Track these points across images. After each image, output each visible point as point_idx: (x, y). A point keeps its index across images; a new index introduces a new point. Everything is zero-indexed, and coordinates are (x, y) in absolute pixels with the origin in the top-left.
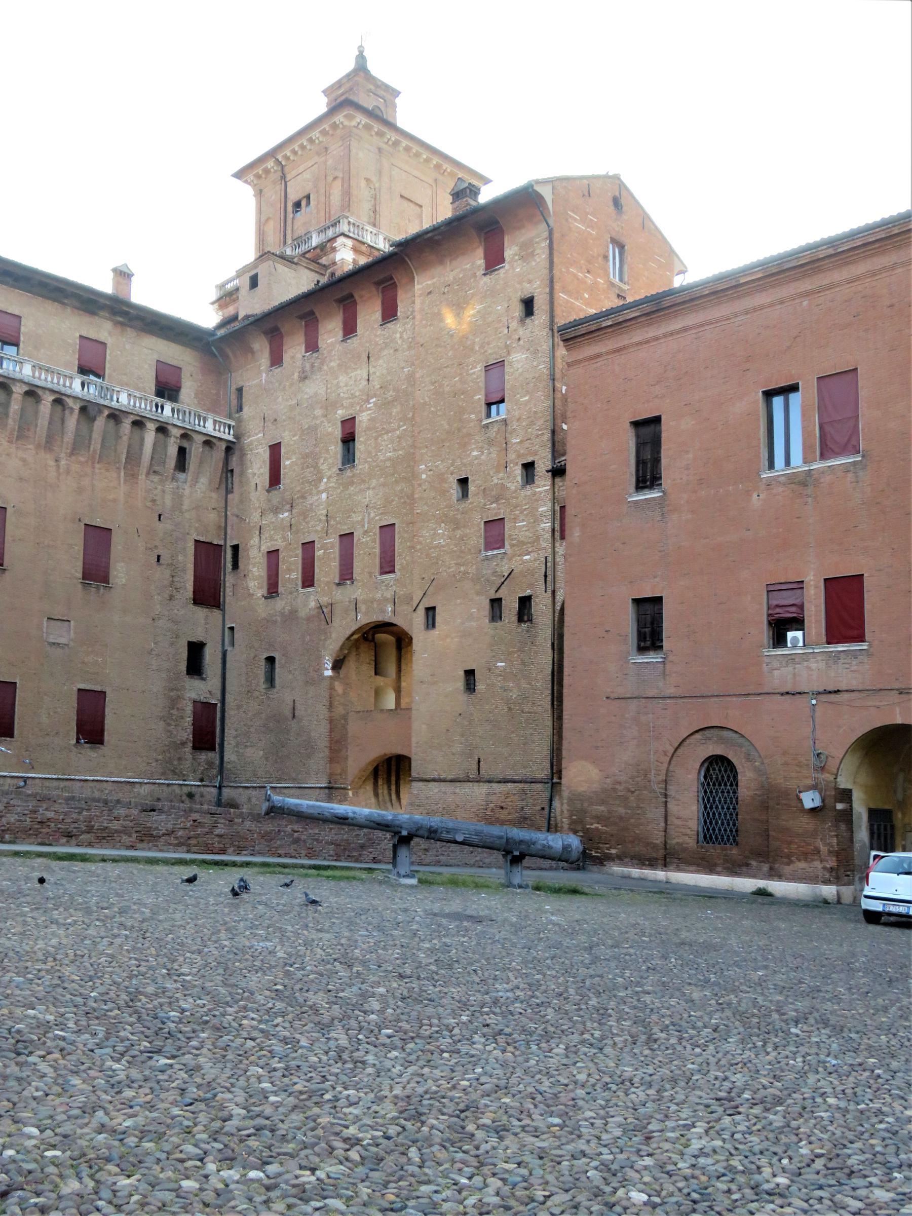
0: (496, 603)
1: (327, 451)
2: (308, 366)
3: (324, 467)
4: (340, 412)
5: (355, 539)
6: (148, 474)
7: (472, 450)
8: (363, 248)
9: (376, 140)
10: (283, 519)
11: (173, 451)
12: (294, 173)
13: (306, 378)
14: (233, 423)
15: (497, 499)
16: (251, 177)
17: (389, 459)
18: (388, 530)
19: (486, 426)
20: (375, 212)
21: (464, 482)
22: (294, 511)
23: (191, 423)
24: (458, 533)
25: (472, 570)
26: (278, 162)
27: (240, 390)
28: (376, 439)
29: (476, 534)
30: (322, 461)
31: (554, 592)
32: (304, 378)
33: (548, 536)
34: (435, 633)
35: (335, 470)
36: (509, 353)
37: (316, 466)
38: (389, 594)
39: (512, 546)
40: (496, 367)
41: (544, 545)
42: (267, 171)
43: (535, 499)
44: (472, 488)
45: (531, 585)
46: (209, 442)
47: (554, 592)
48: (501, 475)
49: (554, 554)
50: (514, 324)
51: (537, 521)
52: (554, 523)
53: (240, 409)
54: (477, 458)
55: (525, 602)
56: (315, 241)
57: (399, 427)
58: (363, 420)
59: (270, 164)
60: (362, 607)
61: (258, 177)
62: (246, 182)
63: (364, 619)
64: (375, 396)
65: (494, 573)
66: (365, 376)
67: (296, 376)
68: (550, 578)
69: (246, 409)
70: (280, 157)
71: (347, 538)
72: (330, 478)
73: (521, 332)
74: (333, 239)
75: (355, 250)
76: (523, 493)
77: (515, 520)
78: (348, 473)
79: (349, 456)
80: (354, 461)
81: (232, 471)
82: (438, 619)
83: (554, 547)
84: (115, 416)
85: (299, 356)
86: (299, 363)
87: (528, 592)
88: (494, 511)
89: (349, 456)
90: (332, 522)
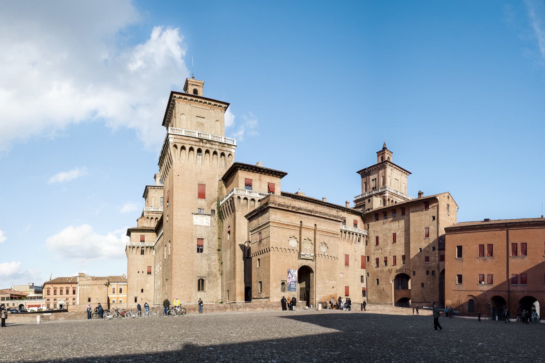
0: (428, 273)
8: (390, 193)
9: (391, 167)
12: (372, 173)
16: (361, 173)
20: (390, 183)
24: (420, 258)
25: (423, 265)
26: (368, 171)
29: (423, 259)
31: (439, 270)
33: (438, 260)
39: (431, 261)
41: (437, 262)
42: (365, 172)
43: (435, 254)
45: (434, 269)
47: (439, 270)
49: (439, 263)
51: (436, 257)
52: (439, 258)
54: (423, 245)
55: (433, 272)
56: (380, 191)
59: (366, 171)
61: (362, 173)
62: (360, 174)
65: (427, 266)
68: (438, 268)
70: (369, 170)
74: (385, 191)
75: (389, 193)
76: (433, 252)
77: (431, 257)
83: (439, 262)
87: (434, 270)
88: (427, 255)
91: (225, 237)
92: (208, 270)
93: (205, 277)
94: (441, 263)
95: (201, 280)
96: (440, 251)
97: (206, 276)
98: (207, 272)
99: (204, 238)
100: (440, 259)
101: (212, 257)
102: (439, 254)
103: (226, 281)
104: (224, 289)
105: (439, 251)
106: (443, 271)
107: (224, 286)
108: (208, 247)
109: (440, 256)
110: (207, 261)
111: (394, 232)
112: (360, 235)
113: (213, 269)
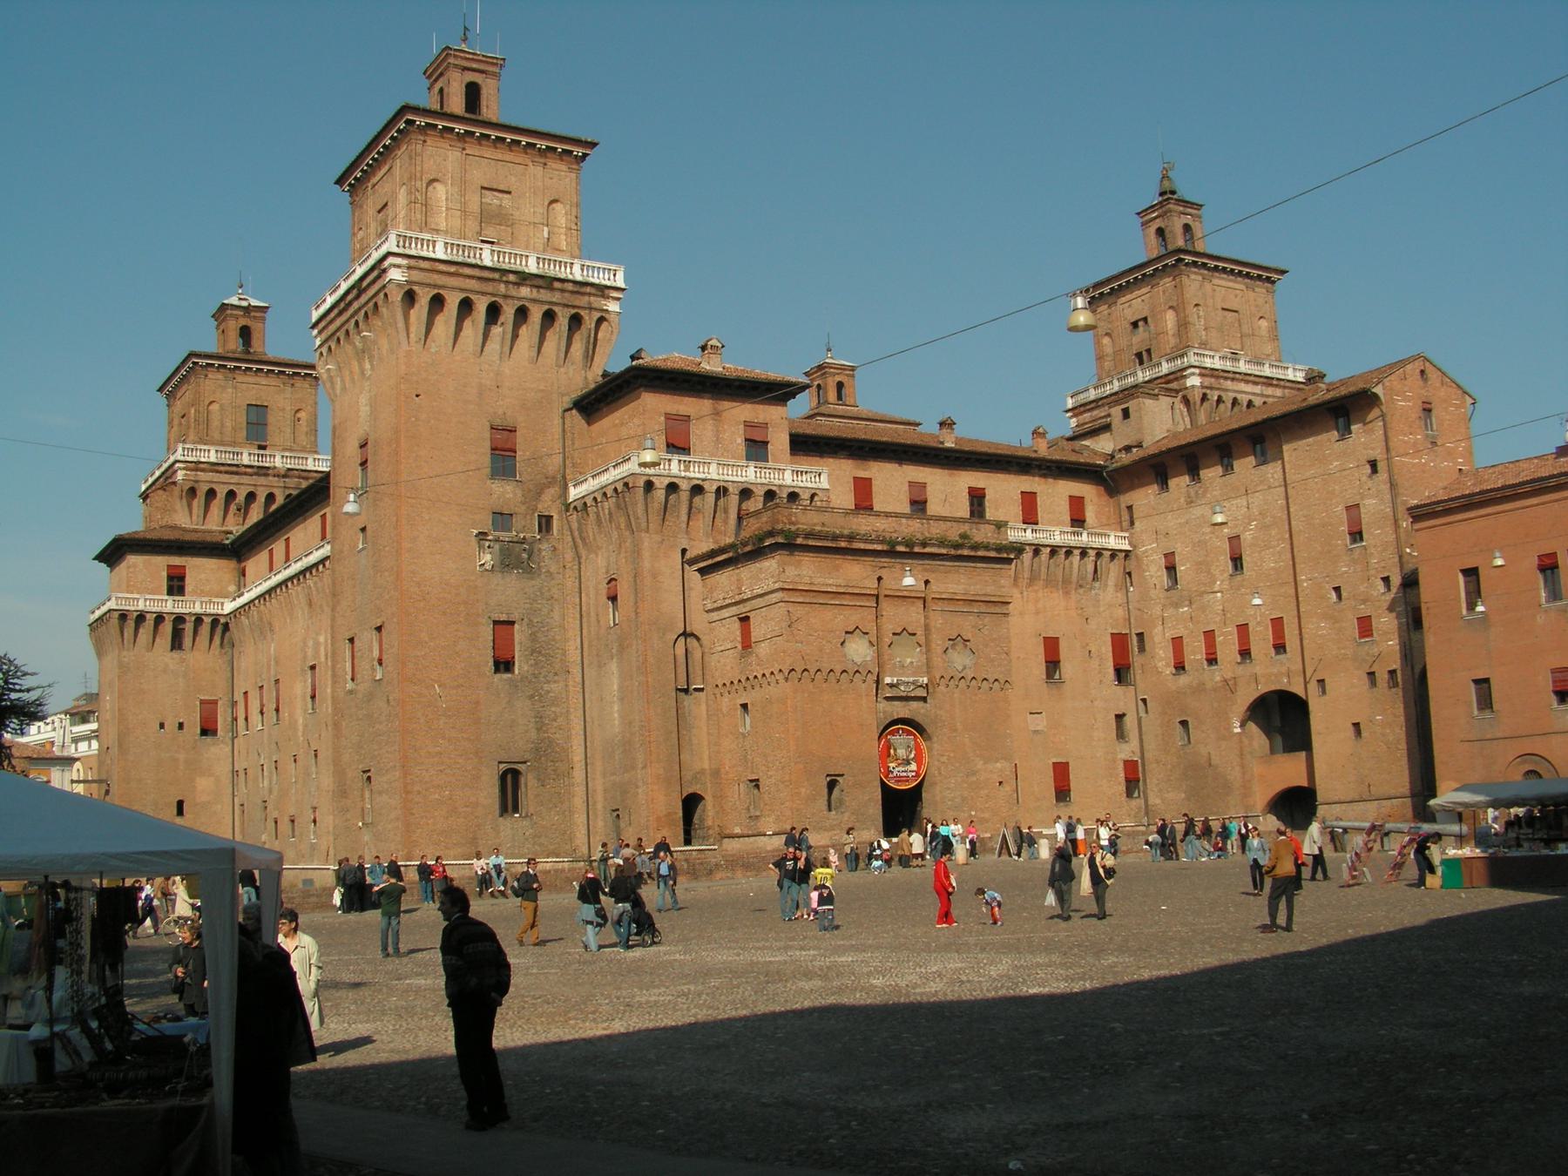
1: (1218, 560)
2: (1193, 493)
3: (1216, 573)
4: (1226, 530)
5: (1250, 629)
6: (1076, 589)
7: (1342, 567)
10: (1183, 613)
11: (1090, 568)
13: (1192, 502)
14: (1127, 535)
15: (1364, 601)
17: (1273, 568)
18: (1277, 623)
19: (1351, 550)
21: (1337, 590)
22: (1194, 606)
23: (1098, 542)
27: (1130, 508)
28: (1260, 552)
30: (1214, 567)
32: (1190, 502)
34: (1326, 697)
35: (1226, 575)
36: (1362, 499)
37: (1209, 572)
38: (1284, 669)
40: (1353, 509)
44: (1344, 594)
46: (1114, 554)
48: (1366, 585)
50: (1364, 478)
52: (1407, 618)
53: (1132, 523)
57: (1279, 545)
58: (1247, 537)
60: (1262, 680)
63: (1263, 688)
64: (1255, 520)
66: (1245, 504)
67: (1182, 500)
69: (1137, 524)
71: (1243, 629)
72: (1222, 581)
73: (1370, 483)
78: (1239, 578)
79: (1237, 561)
80: (1242, 568)
81: (1129, 574)
82: (1327, 687)
84: (1054, 550)
85: (1183, 485)
86: (1184, 490)
89: (1237, 561)
90: (1229, 615)
91: (592, 614)
92: (533, 735)
93: (525, 762)
94: (1415, 636)
95: (509, 776)
96: (1408, 590)
97: (527, 757)
98: (533, 742)
99: (515, 616)
100: (1410, 621)
101: (546, 687)
102: (1406, 603)
103: (604, 777)
104: (599, 806)
105: (1405, 593)
106: (1425, 667)
107: (595, 791)
108: (533, 651)
109: (1409, 609)
110: (528, 703)
111: (1234, 532)
112: (1099, 554)
113: (553, 731)
